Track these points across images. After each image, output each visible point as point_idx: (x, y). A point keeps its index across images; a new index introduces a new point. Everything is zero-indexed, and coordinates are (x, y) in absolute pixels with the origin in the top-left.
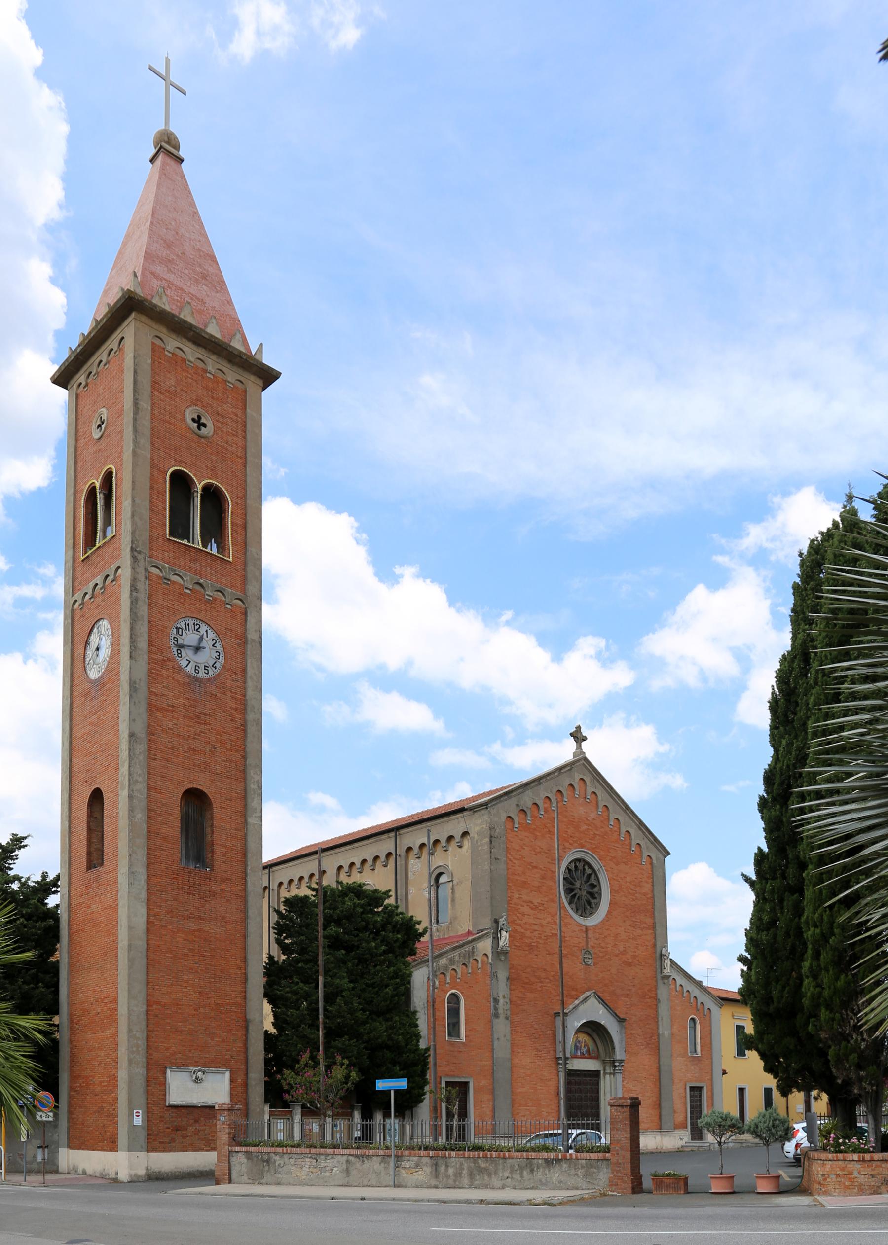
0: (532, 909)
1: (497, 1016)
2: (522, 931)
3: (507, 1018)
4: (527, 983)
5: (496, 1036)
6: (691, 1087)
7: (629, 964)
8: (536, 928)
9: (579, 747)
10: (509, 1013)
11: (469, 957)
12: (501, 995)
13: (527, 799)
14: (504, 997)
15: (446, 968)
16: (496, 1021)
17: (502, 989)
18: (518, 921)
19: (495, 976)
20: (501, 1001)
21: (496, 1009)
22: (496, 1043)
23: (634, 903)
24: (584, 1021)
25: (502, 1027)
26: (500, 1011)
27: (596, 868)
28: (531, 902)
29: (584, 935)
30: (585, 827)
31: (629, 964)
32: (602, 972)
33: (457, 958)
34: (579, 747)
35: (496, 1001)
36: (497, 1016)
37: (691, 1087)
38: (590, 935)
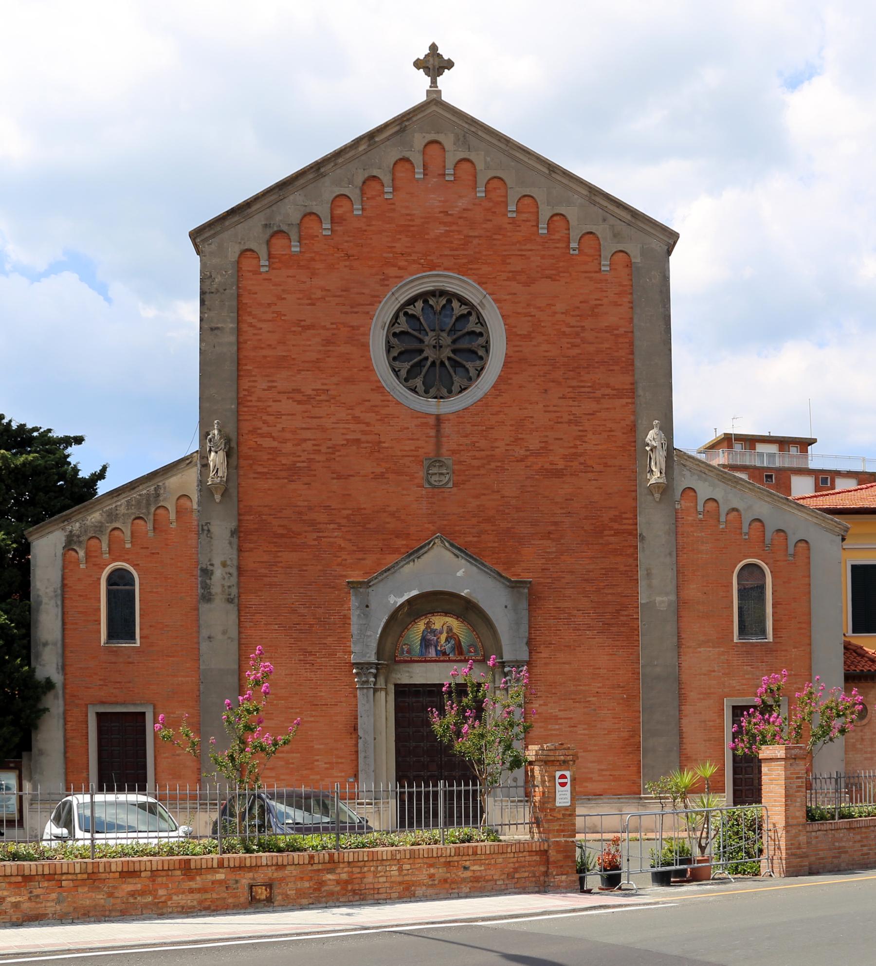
0: (299, 402)
1: (207, 598)
2: (275, 444)
3: (230, 601)
4: (282, 536)
5: (204, 633)
6: (734, 708)
7: (558, 474)
8: (308, 434)
9: (434, 83)
10: (234, 591)
11: (148, 504)
12: (217, 561)
13: (290, 210)
14: (224, 565)
15: (99, 528)
16: (204, 607)
17: (221, 550)
18: (265, 429)
19: (205, 530)
20: (218, 573)
21: (206, 586)
22: (204, 646)
23: (575, 351)
24: (415, 593)
25: (219, 618)
26: (216, 589)
27: (475, 301)
28: (298, 391)
29: (432, 433)
30: (442, 229)
31: (558, 474)
32: (477, 497)
33: (123, 510)
34: (434, 83)
35: (207, 573)
36: (207, 598)
37: (734, 708)
38: (447, 429)
